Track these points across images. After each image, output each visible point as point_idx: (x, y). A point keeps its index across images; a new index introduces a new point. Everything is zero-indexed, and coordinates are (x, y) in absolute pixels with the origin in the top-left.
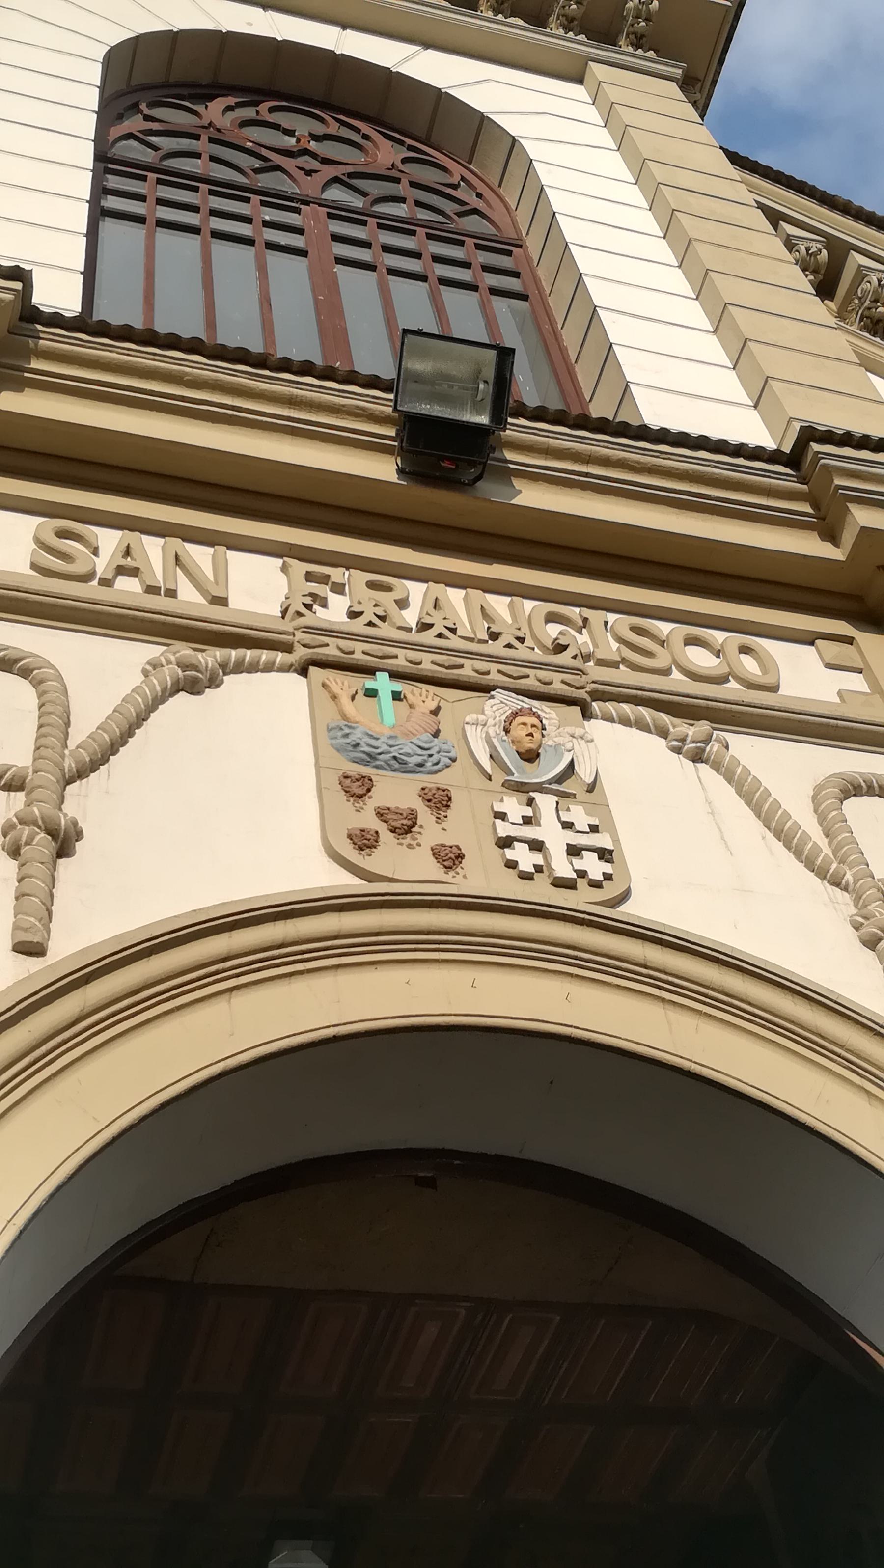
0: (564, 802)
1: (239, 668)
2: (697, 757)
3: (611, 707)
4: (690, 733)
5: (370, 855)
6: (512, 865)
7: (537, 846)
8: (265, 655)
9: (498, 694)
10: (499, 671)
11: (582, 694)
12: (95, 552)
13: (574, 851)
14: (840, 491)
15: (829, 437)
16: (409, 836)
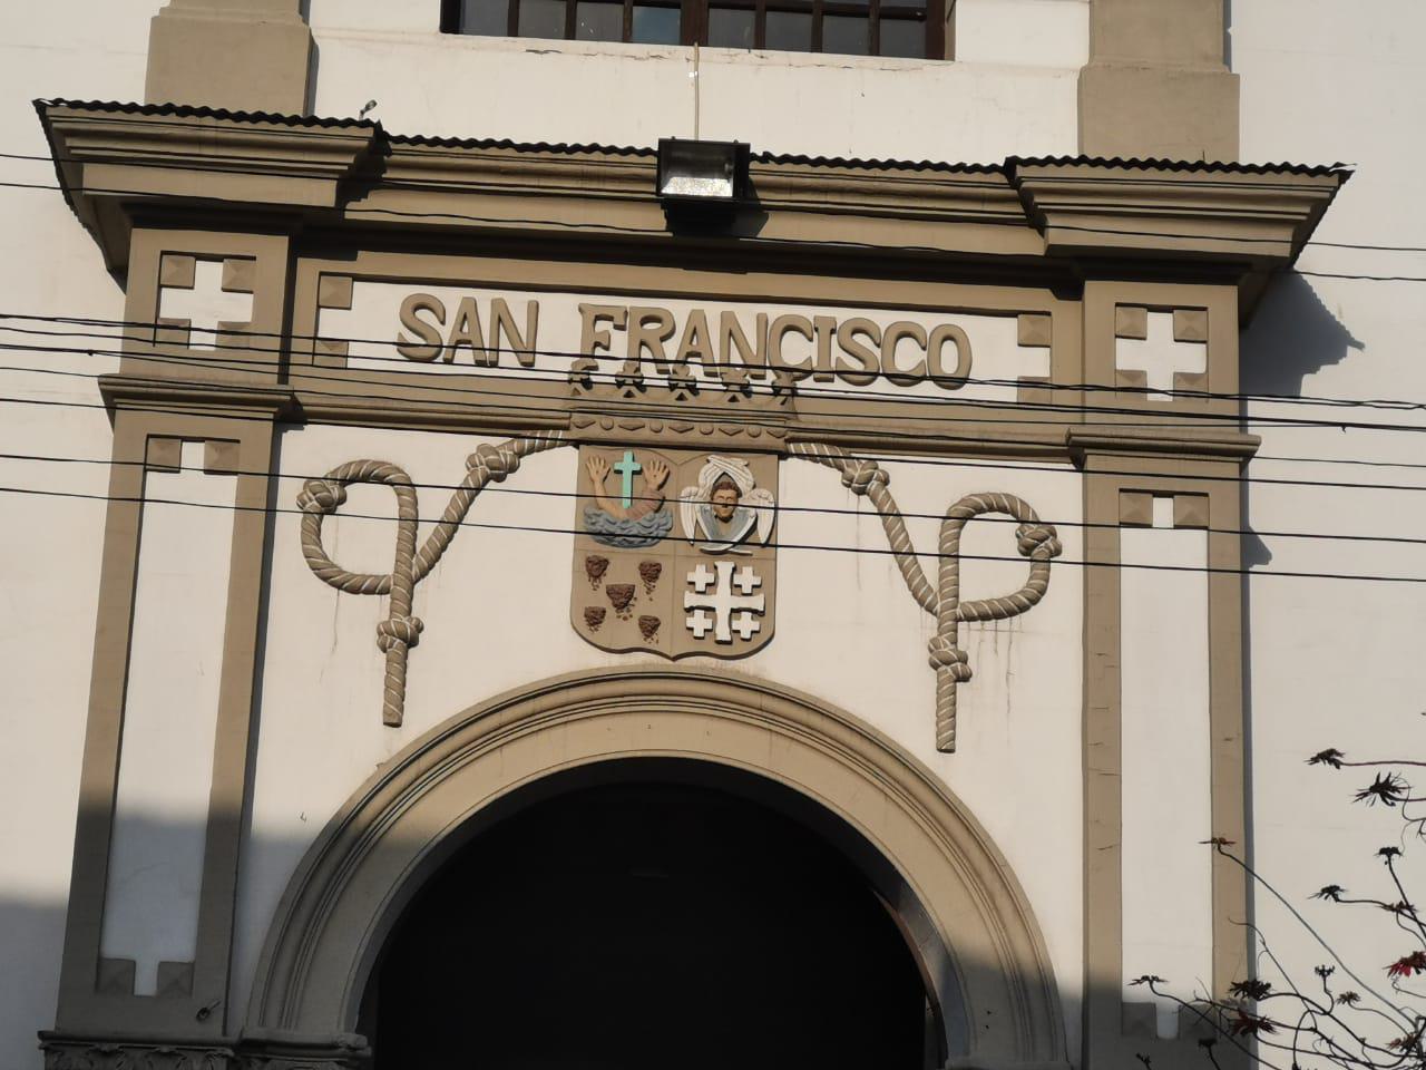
0: (740, 561)
1: (531, 451)
2: (860, 492)
3: (803, 448)
4: (856, 475)
5: (596, 630)
6: (691, 629)
7: (709, 610)
8: (550, 434)
9: (714, 458)
10: (720, 430)
11: (779, 444)
12: (443, 323)
13: (735, 612)
14: (1040, 207)
15: (1032, 161)
16: (625, 609)
